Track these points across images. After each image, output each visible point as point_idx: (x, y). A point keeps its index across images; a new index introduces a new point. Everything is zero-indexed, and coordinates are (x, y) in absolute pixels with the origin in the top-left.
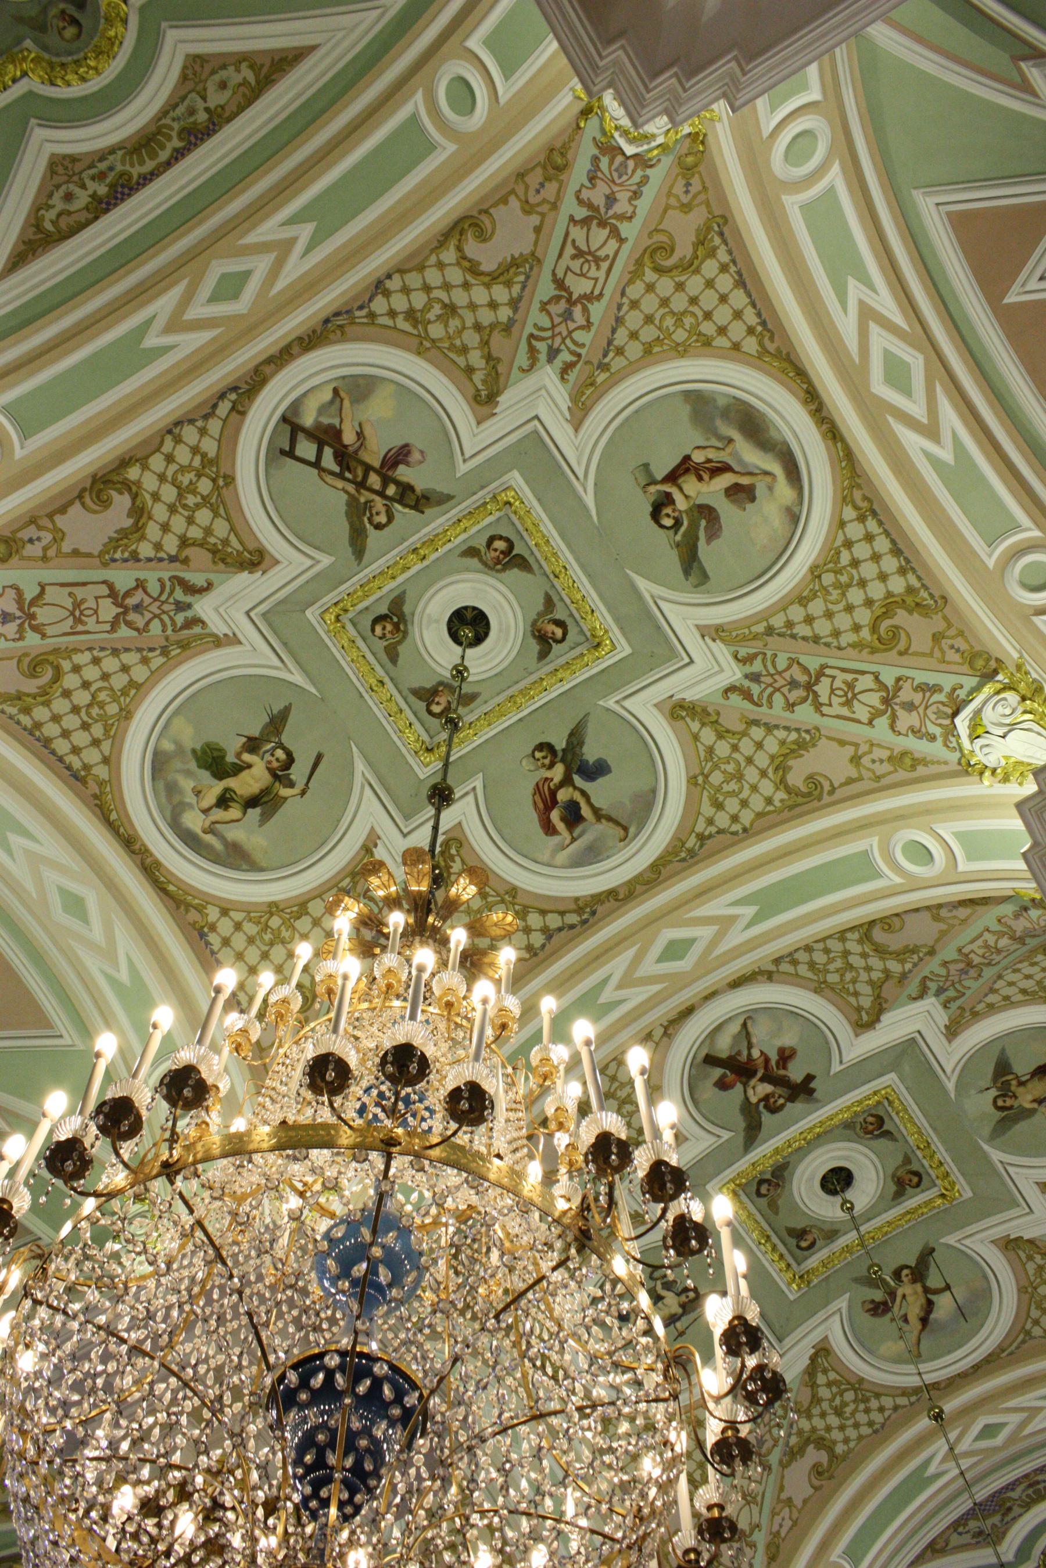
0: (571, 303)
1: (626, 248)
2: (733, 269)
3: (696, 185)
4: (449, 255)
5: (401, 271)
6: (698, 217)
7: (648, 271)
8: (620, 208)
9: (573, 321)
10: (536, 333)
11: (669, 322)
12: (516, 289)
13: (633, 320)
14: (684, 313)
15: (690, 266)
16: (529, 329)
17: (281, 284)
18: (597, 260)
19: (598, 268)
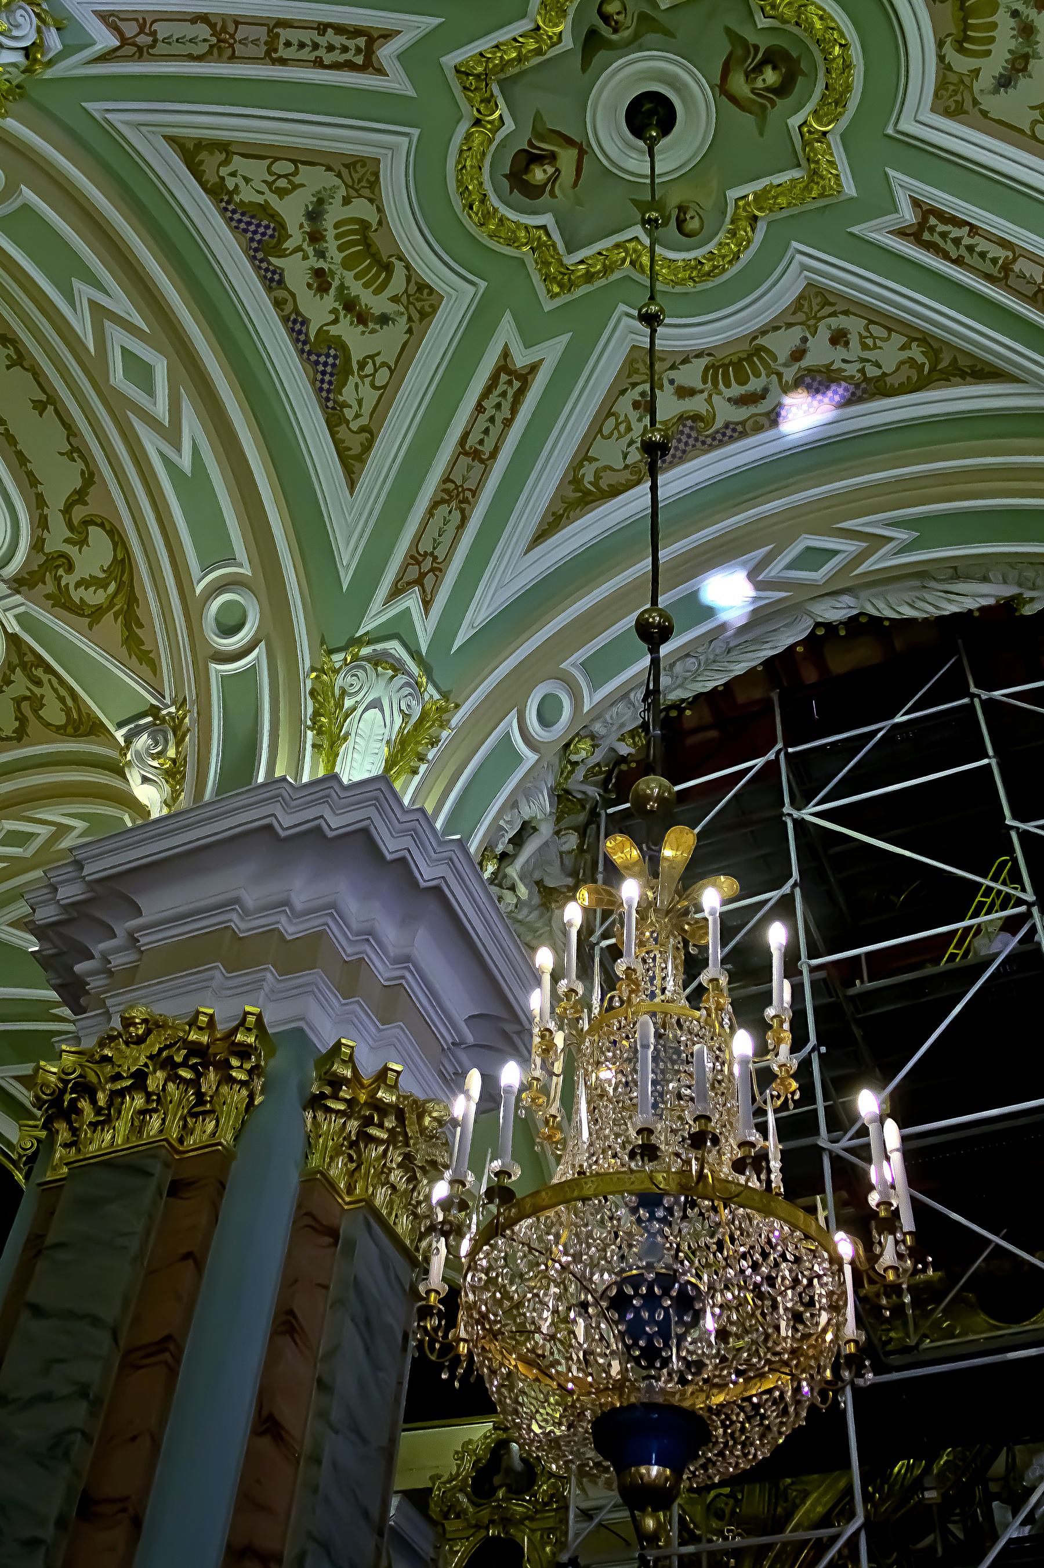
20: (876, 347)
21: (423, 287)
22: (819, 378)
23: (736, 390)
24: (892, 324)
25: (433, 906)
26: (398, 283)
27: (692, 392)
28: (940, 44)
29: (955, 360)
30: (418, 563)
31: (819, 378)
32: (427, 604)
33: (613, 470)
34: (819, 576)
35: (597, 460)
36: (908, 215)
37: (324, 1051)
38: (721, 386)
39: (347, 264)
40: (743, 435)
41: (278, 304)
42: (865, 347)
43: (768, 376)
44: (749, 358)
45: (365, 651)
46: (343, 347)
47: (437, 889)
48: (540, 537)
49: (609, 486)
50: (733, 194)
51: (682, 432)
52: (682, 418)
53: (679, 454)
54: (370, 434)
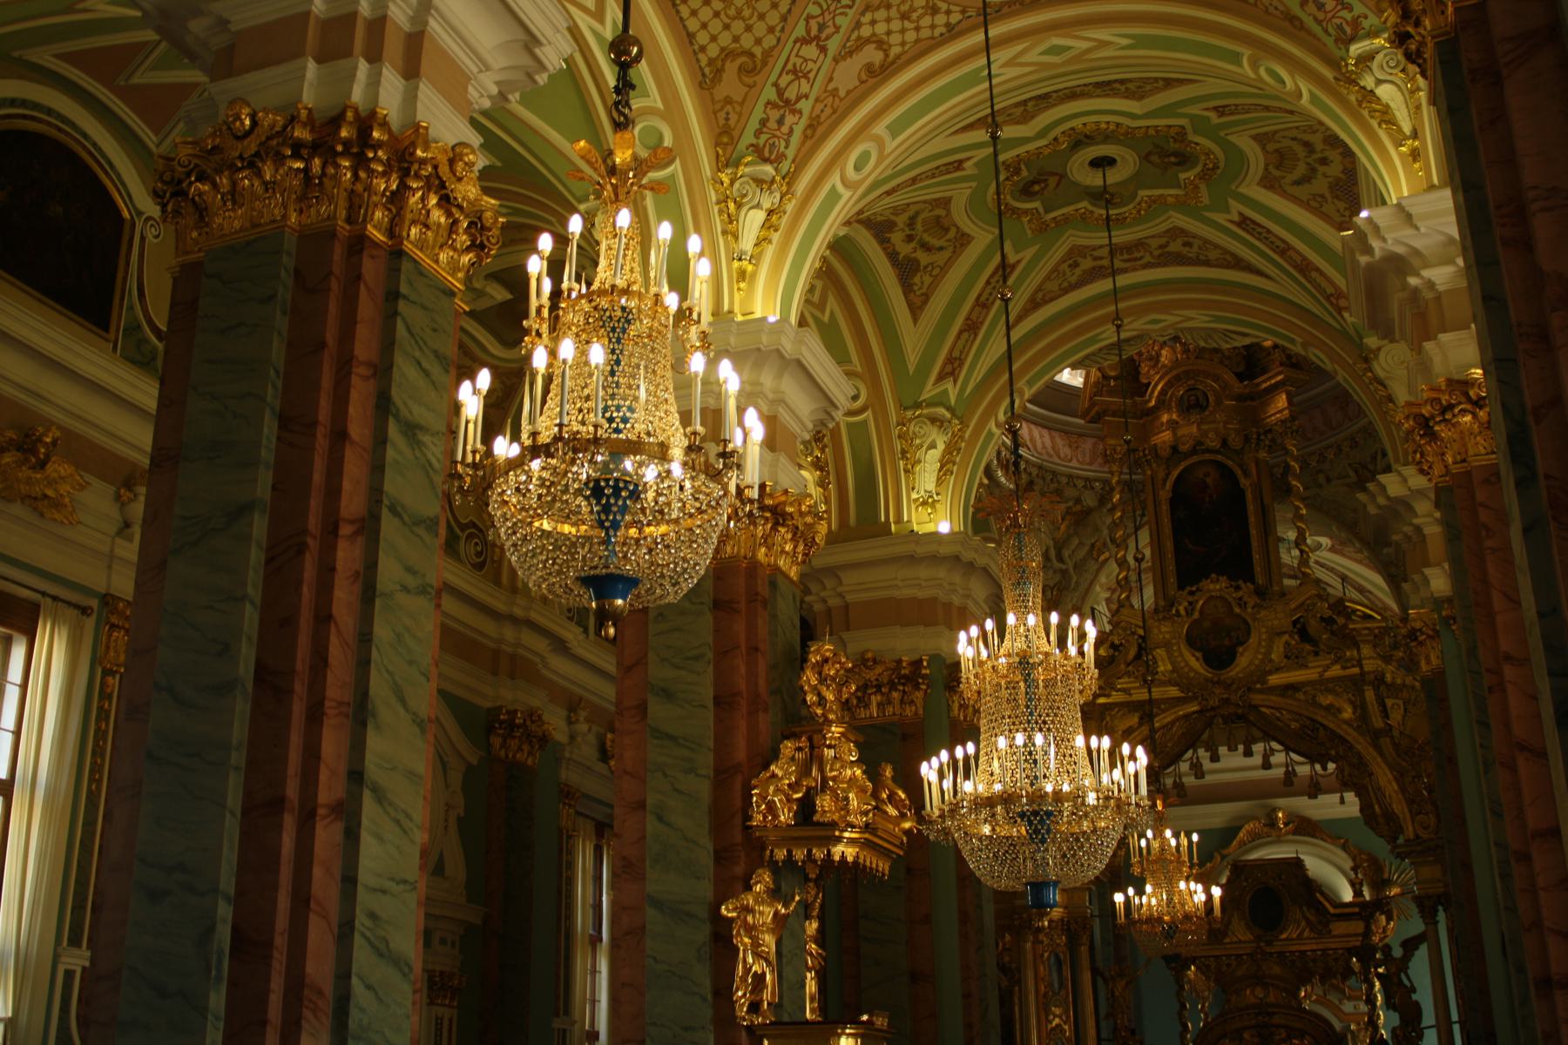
0: (817, 38)
1: (773, 78)
2: (696, 47)
3: (722, 115)
4: (895, 50)
5: (932, 38)
6: (721, 91)
7: (759, 56)
8: (774, 114)
9: (819, 24)
10: (847, 10)
11: (746, 13)
12: (854, 37)
13: (773, 18)
14: (734, 19)
15: (727, 54)
16: (850, 12)
17: (1019, 48)
18: (794, 71)
19: (794, 65)
21: (964, 235)
23: (1126, 257)
24: (1216, 246)
26: (952, 234)
27: (1101, 258)
28: (1267, 165)
32: (955, 382)
36: (1236, 218)
39: (924, 231)
41: (884, 249)
44: (1136, 246)
46: (917, 261)
50: (1143, 193)
52: (1094, 268)
54: (926, 297)
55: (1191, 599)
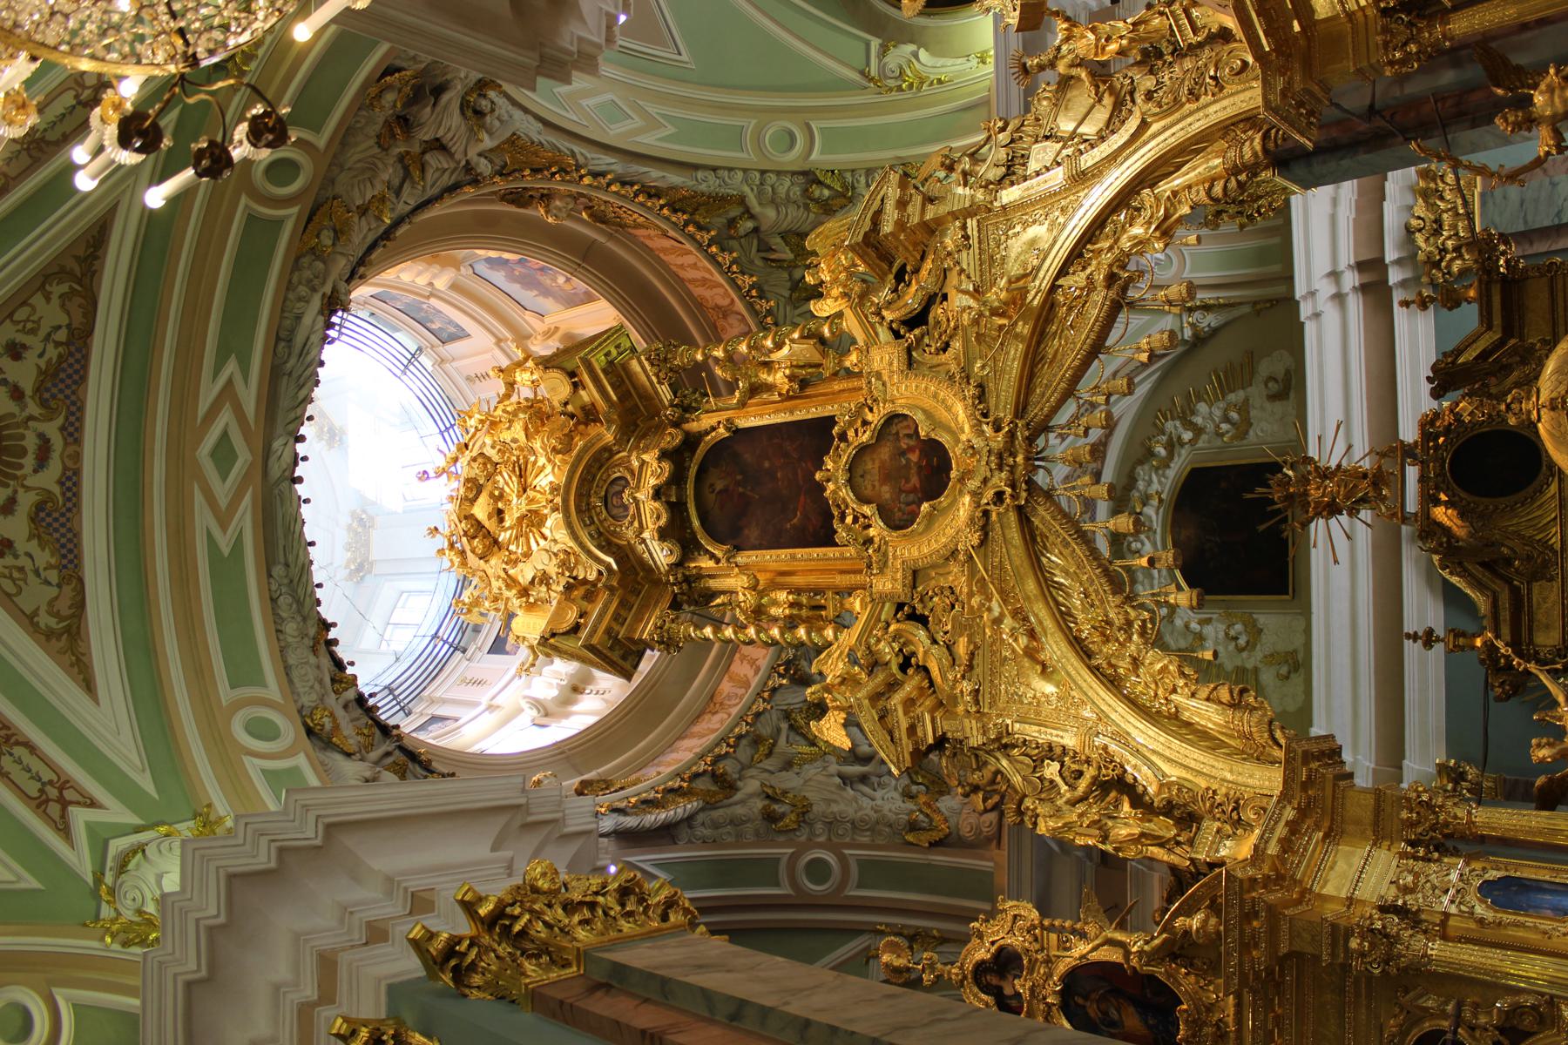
20: (38, 322)
22: (49, 385)
23: (29, 462)
25: (349, 841)
29: (77, 258)
30: (48, 801)
31: (49, 385)
32: (92, 804)
33: (56, 598)
34: (244, 457)
35: (38, 609)
37: (424, 973)
38: (19, 473)
40: (77, 472)
42: (33, 332)
43: (27, 428)
45: (109, 878)
47: (331, 829)
48: (89, 686)
49: (70, 608)
51: (49, 525)
52: (34, 519)
53: (70, 535)
55: (849, 520)
